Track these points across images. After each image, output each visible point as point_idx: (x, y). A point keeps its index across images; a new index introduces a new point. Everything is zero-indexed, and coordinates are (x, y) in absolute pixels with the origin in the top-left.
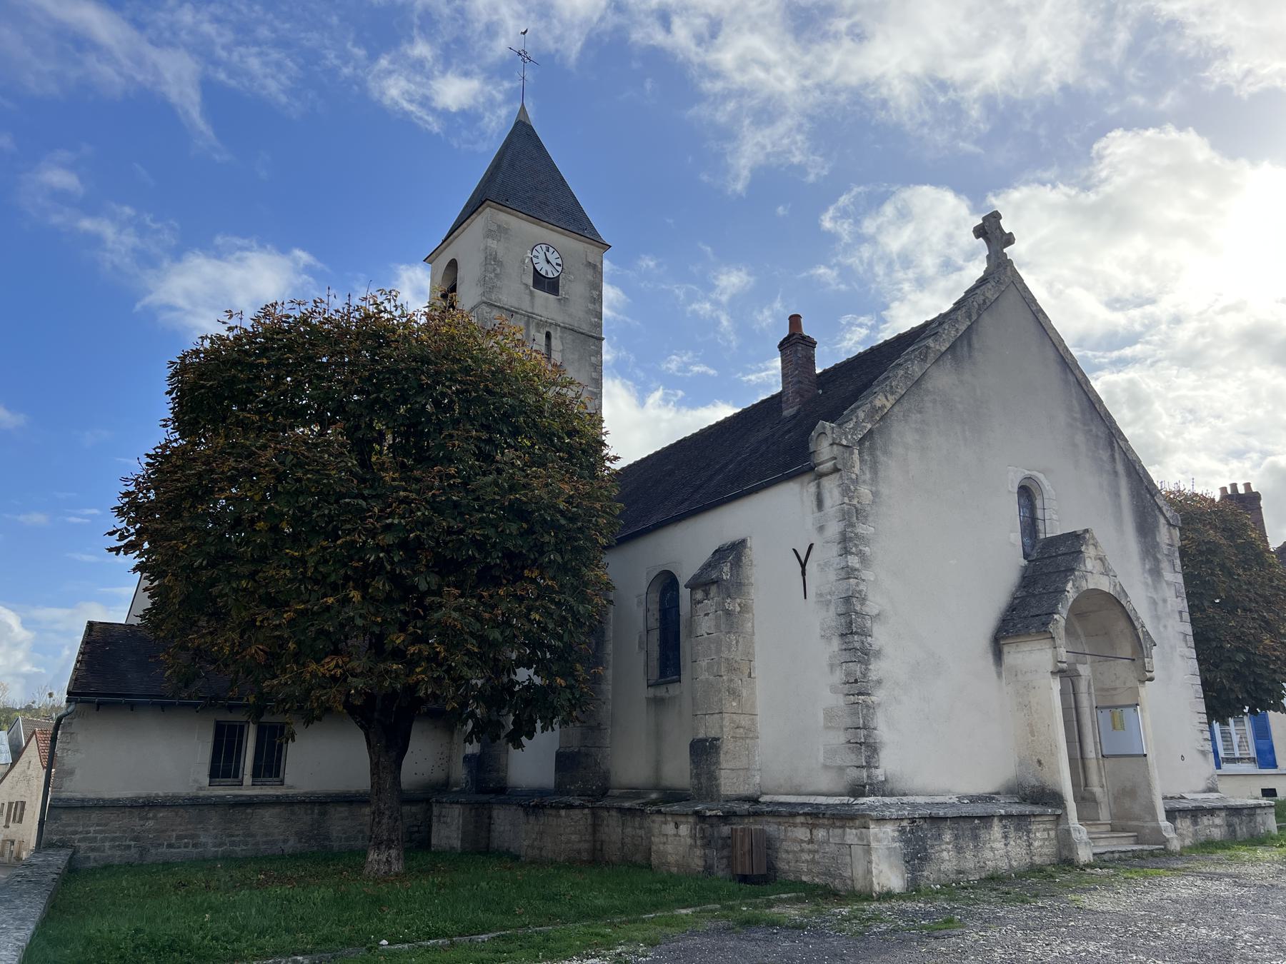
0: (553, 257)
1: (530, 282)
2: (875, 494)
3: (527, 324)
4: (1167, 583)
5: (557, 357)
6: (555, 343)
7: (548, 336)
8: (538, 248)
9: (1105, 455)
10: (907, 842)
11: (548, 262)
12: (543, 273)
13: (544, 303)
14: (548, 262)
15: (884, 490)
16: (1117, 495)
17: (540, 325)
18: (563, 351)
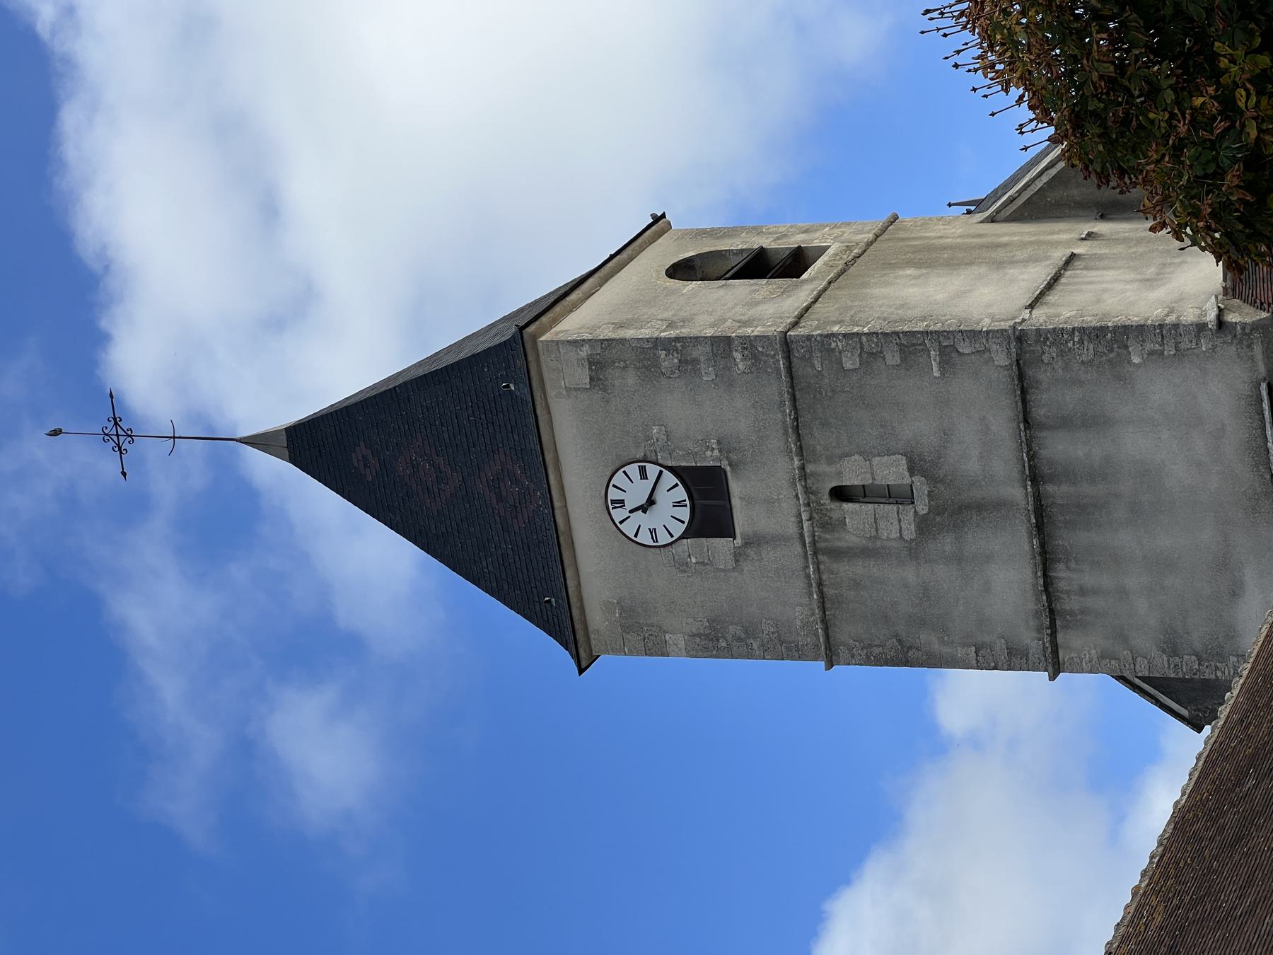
0: (636, 492)
1: (721, 546)
3: (838, 554)
5: (892, 472)
7: (841, 494)
8: (628, 528)
11: (651, 502)
12: (685, 513)
13: (763, 500)
14: (651, 502)
17: (827, 524)
18: (866, 455)
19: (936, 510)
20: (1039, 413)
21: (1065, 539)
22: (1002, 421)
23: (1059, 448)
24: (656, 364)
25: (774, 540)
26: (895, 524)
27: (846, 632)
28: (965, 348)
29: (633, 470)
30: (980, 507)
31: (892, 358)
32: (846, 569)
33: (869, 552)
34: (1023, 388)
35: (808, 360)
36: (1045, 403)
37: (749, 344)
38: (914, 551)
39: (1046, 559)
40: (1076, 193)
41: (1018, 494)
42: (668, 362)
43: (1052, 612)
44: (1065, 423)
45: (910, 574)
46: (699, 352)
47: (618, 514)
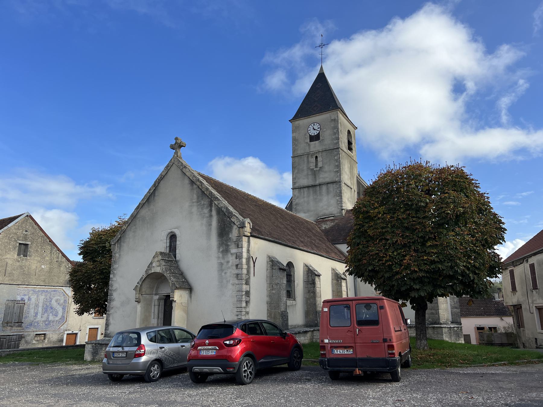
0: (316, 127)
2: (120, 255)
3: (308, 157)
4: (232, 254)
5: (320, 164)
6: (319, 159)
7: (316, 157)
8: (310, 126)
9: (206, 211)
10: (94, 349)
12: (313, 135)
13: (315, 146)
15: (122, 253)
16: (210, 225)
18: (322, 161)
19: (315, 171)
20: (329, 185)
21: (311, 189)
22: (328, 180)
23: (324, 188)
24: (335, 129)
25: (309, 148)
26: (312, 166)
27: (296, 159)
28: (338, 174)
29: (319, 127)
30: (315, 177)
31: (336, 164)
32: (306, 159)
33: (308, 162)
34: (332, 183)
35: (336, 151)
36: (331, 186)
37: (338, 143)
38: (308, 168)
39: (308, 187)
40: (361, 189)
41: (317, 183)
42: (335, 131)
43: (300, 188)
44: (328, 189)
45: (305, 168)
46: (337, 135)
47: (312, 125)
